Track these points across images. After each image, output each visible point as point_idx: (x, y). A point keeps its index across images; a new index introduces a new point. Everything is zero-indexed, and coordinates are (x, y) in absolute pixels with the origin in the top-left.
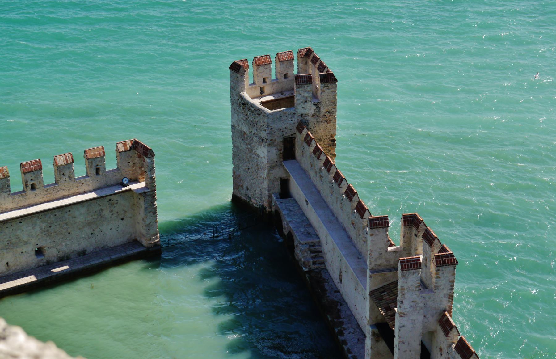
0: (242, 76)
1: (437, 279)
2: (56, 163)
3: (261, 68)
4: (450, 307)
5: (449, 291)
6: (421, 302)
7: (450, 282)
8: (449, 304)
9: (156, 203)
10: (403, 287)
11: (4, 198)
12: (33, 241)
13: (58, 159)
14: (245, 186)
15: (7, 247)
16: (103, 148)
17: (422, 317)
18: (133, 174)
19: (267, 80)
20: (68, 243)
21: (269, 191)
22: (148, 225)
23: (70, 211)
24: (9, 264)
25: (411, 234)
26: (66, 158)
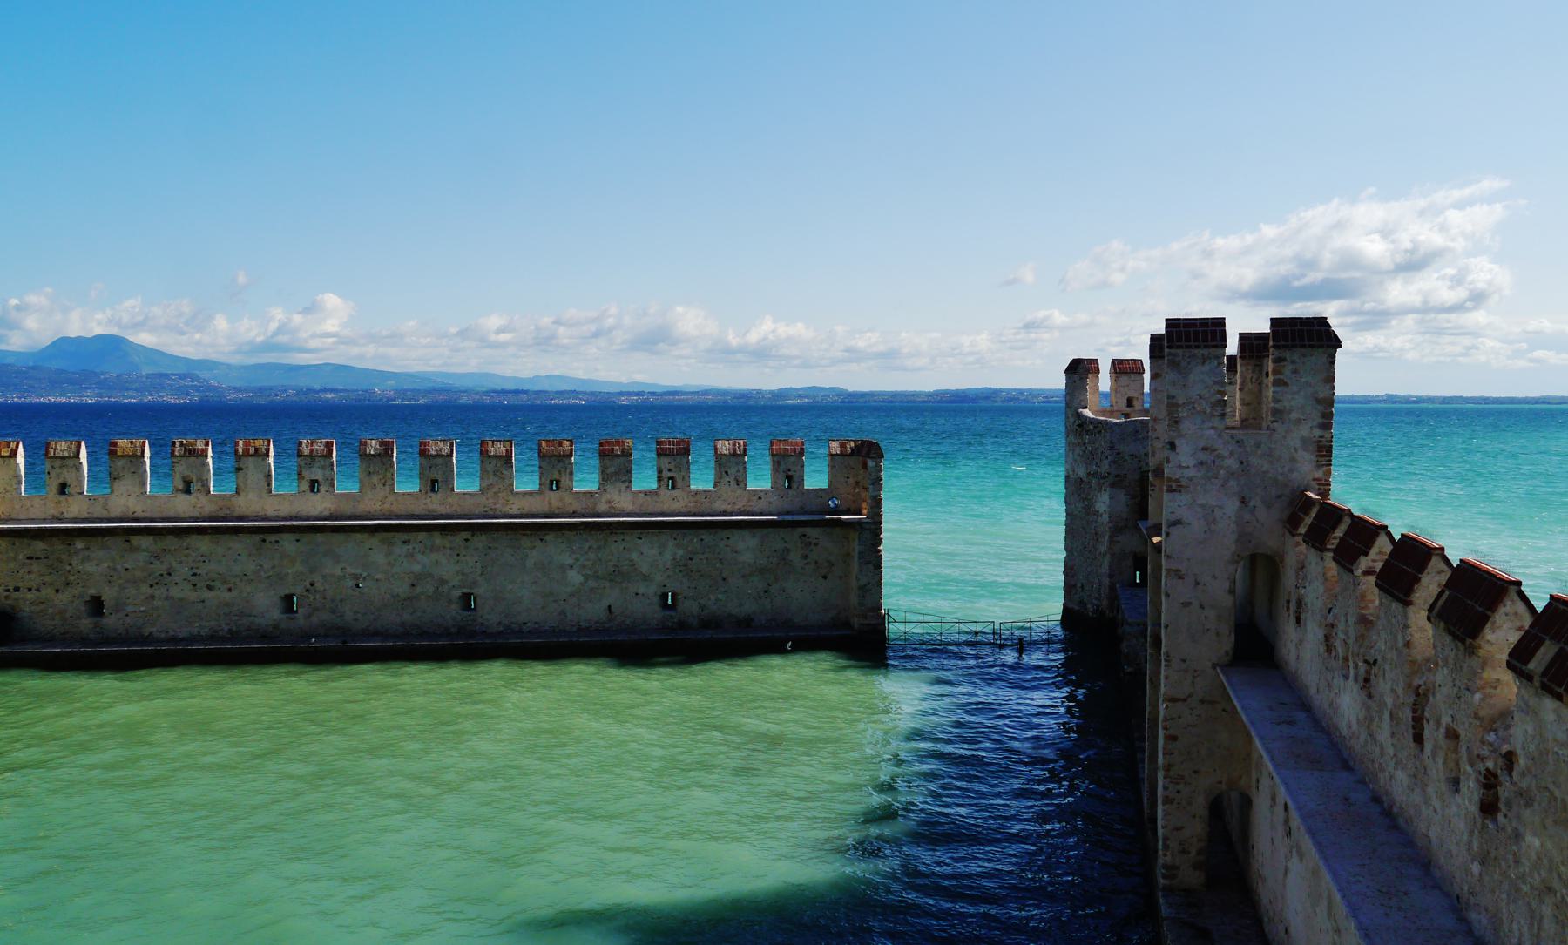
0: (1084, 379)
1: (1278, 389)
2: (716, 449)
3: (1124, 379)
4: (1323, 484)
5: (1317, 433)
6: (1232, 454)
7: (1319, 401)
8: (1319, 474)
9: (881, 548)
10: (1173, 397)
11: (620, 491)
12: (659, 578)
13: (719, 444)
14: (1079, 585)
15: (612, 577)
16: (803, 443)
17: (1237, 504)
18: (854, 502)
19: (1135, 403)
20: (720, 596)
21: (1111, 576)
22: (863, 589)
23: (728, 538)
24: (612, 608)
25: (1260, 384)
26: (734, 445)
